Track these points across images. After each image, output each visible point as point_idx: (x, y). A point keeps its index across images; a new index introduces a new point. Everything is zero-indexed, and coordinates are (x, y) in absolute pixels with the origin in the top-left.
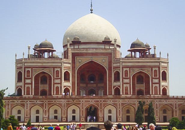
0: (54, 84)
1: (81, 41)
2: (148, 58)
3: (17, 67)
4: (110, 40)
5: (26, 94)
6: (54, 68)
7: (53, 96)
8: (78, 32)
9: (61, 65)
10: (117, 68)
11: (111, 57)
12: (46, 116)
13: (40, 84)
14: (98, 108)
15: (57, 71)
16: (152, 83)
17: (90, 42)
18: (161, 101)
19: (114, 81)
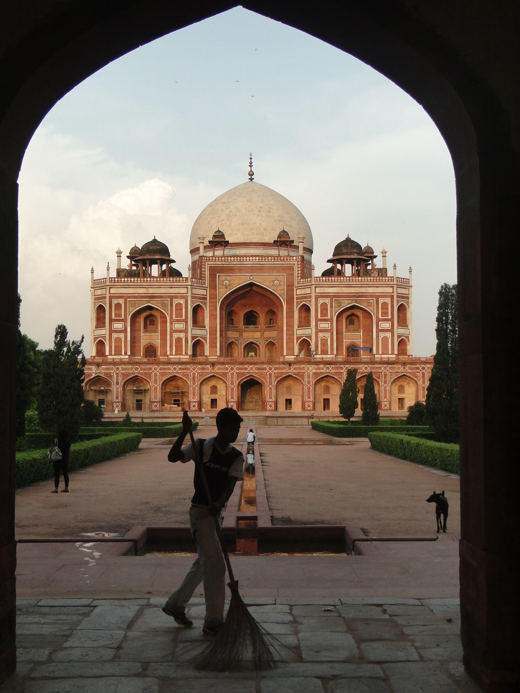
0: (172, 331)
2: (369, 278)
4: (291, 239)
5: (113, 353)
6: (172, 298)
7: (171, 357)
8: (222, 220)
9: (186, 292)
10: (305, 297)
11: (293, 274)
14: (264, 383)
15: (179, 305)
16: (379, 331)
17: (248, 241)
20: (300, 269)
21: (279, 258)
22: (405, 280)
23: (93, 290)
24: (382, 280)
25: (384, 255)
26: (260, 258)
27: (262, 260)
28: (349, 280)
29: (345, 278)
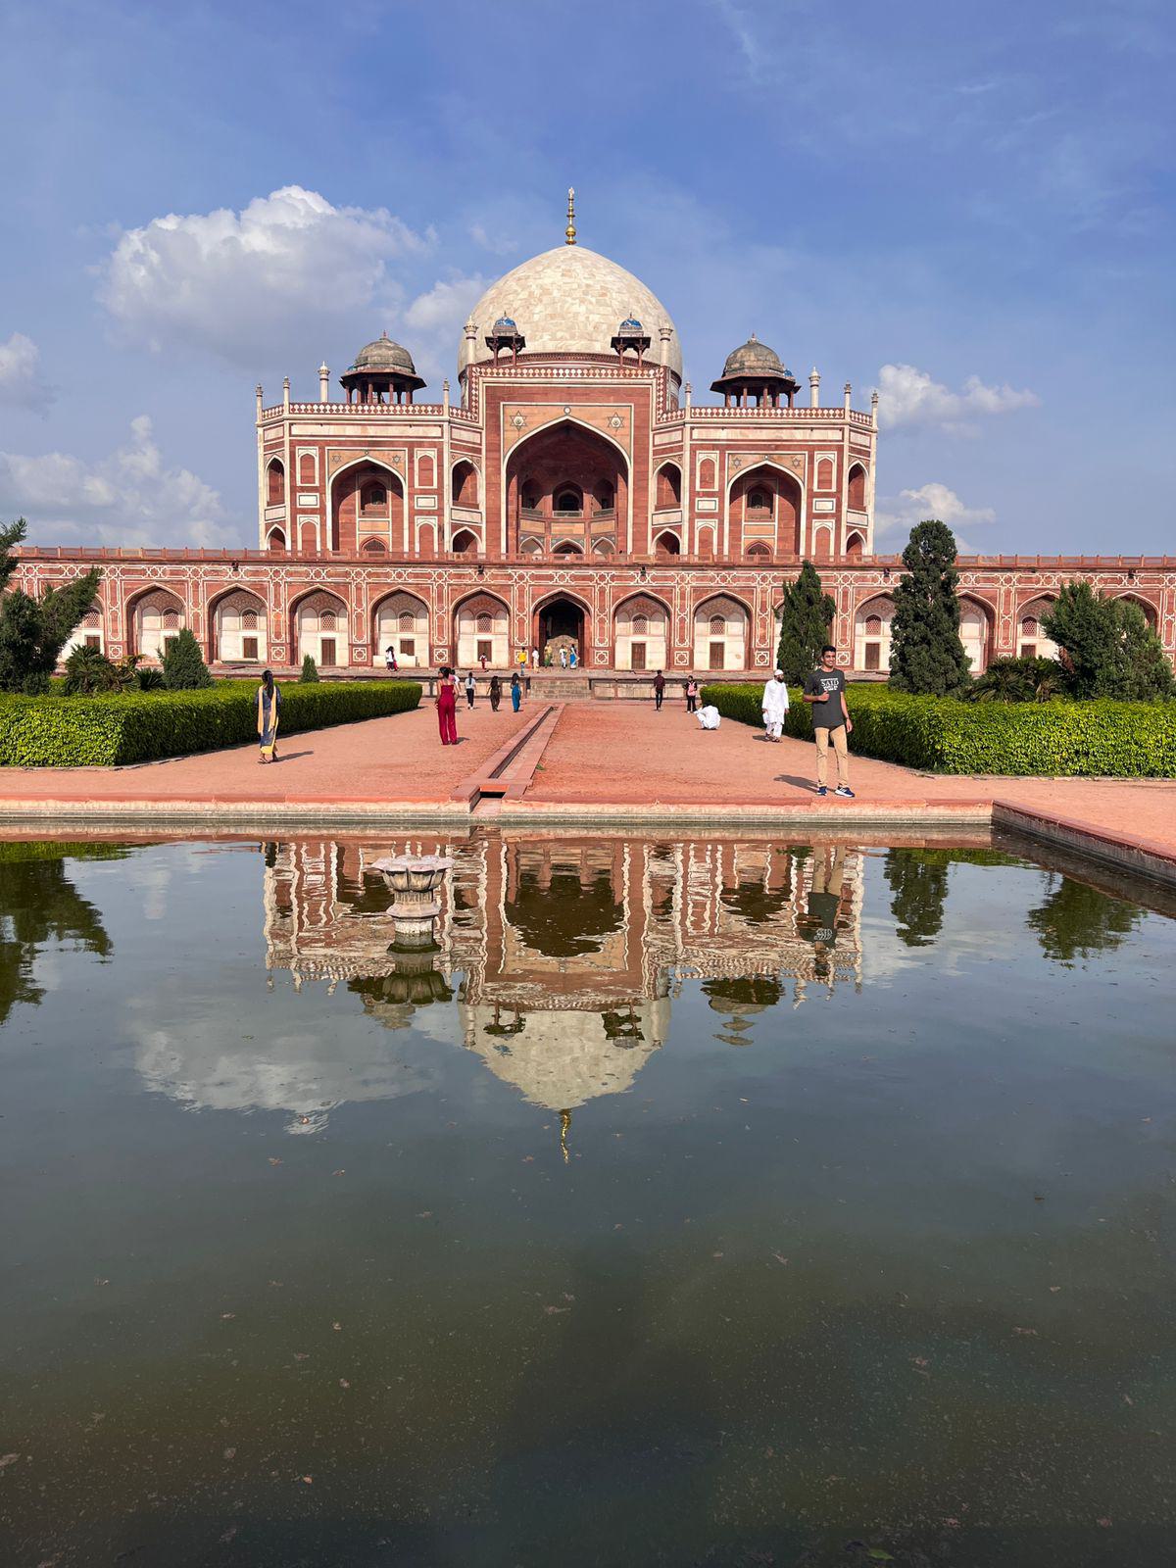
0: (413, 513)
1: (521, 342)
2: (797, 412)
3: (261, 445)
6: (411, 446)
9: (440, 435)
10: (671, 450)
11: (647, 405)
12: (360, 637)
13: (360, 517)
14: (588, 610)
15: (426, 460)
16: (811, 516)
17: (562, 351)
18: (864, 579)
19: (656, 509)
20: (661, 393)
21: (622, 372)
22: (864, 418)
23: (260, 431)
24: (823, 414)
25: (815, 383)
26: (585, 372)
27: (588, 375)
28: (758, 414)
29: (750, 411)
